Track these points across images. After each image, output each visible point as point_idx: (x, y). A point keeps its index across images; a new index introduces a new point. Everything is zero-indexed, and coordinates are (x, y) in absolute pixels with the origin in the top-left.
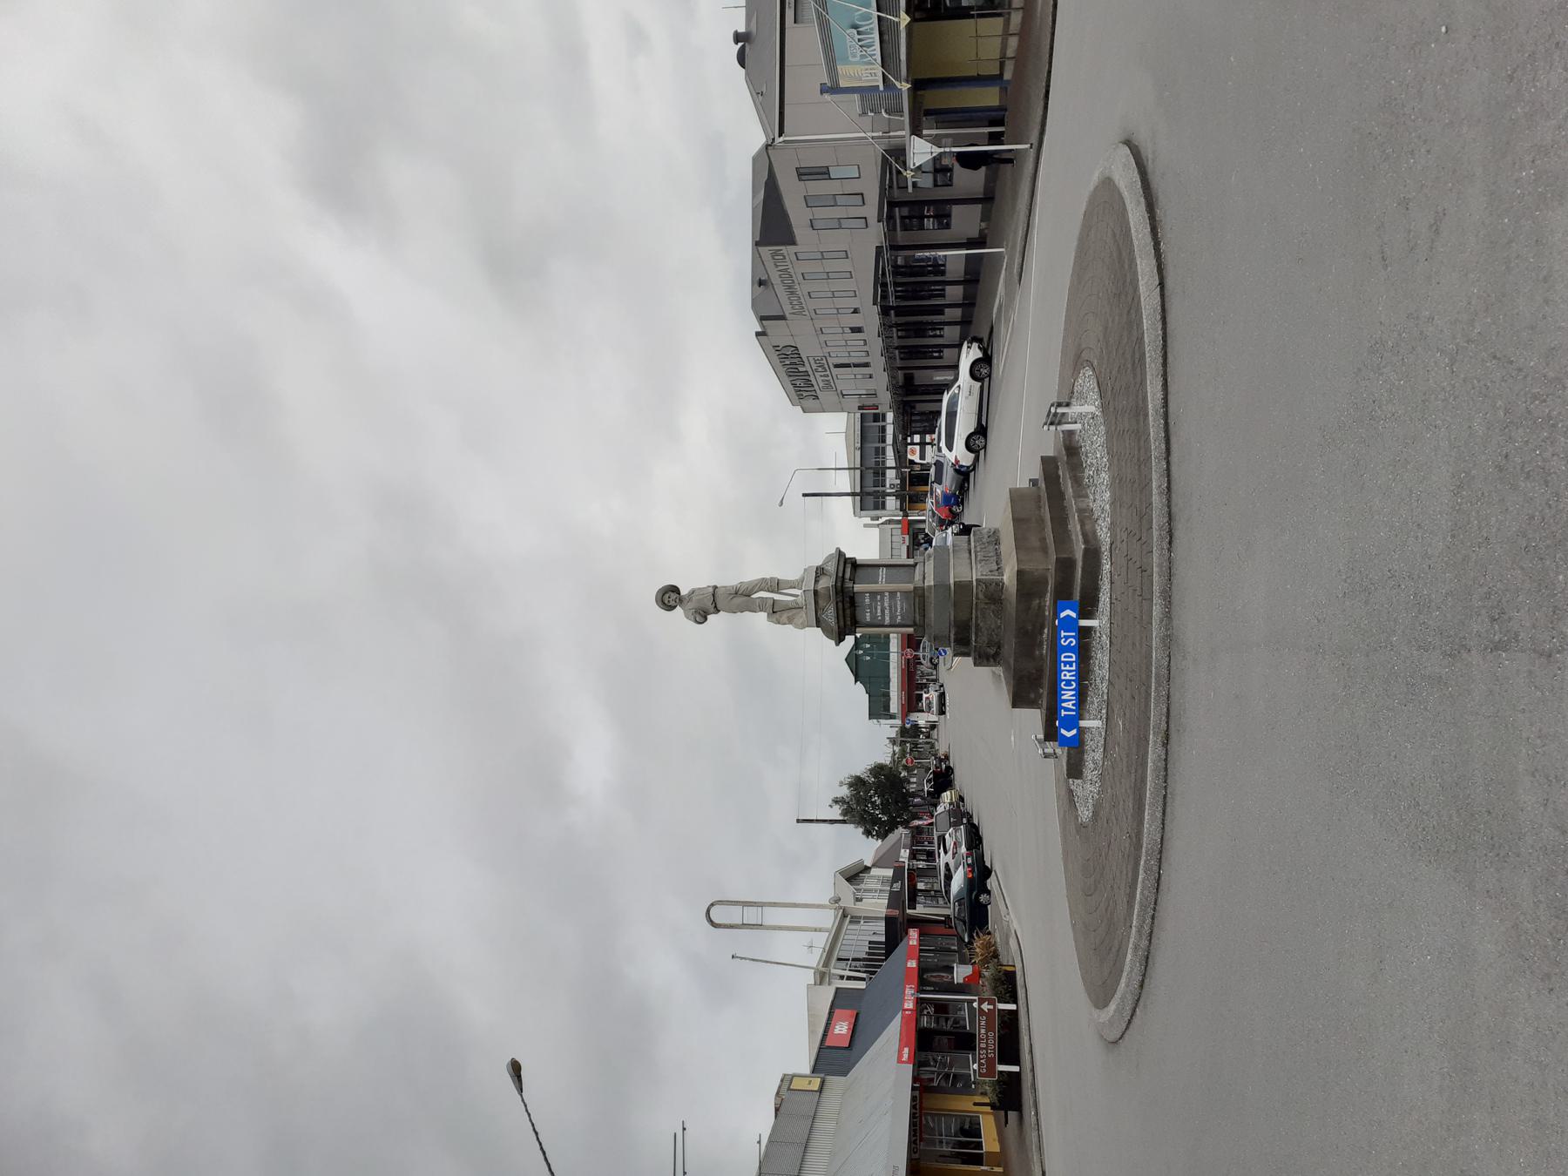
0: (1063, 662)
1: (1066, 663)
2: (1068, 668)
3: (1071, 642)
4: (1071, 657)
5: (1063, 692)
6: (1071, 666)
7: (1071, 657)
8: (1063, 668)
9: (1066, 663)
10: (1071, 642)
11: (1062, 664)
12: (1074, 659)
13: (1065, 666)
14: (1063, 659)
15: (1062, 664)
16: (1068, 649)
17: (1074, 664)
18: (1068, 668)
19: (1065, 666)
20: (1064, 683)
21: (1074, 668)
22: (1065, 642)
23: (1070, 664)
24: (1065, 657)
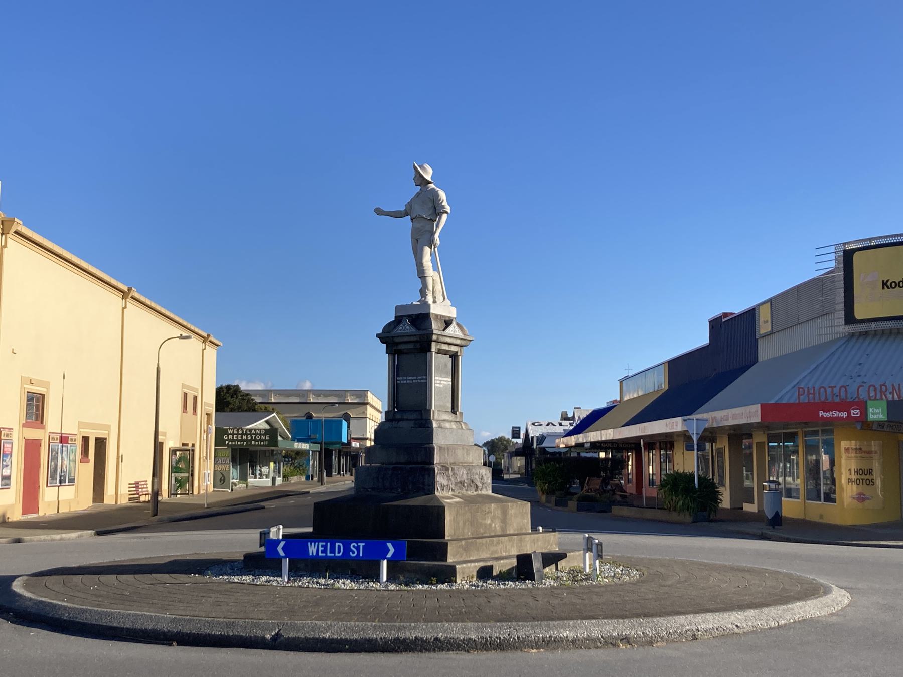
0: (326, 545)
1: (325, 547)
2: (320, 549)
3: (353, 552)
4: (339, 552)
5: (316, 543)
6: (322, 552)
7: (339, 552)
8: (320, 544)
9: (325, 547)
10: (353, 552)
11: (324, 543)
12: (337, 554)
13: (322, 546)
14: (337, 544)
15: (324, 543)
16: (347, 550)
17: (324, 554)
18: (320, 549)
19: (322, 546)
20: (356, 545)
21: (320, 554)
22: (354, 546)
23: (324, 551)
24: (339, 547)
